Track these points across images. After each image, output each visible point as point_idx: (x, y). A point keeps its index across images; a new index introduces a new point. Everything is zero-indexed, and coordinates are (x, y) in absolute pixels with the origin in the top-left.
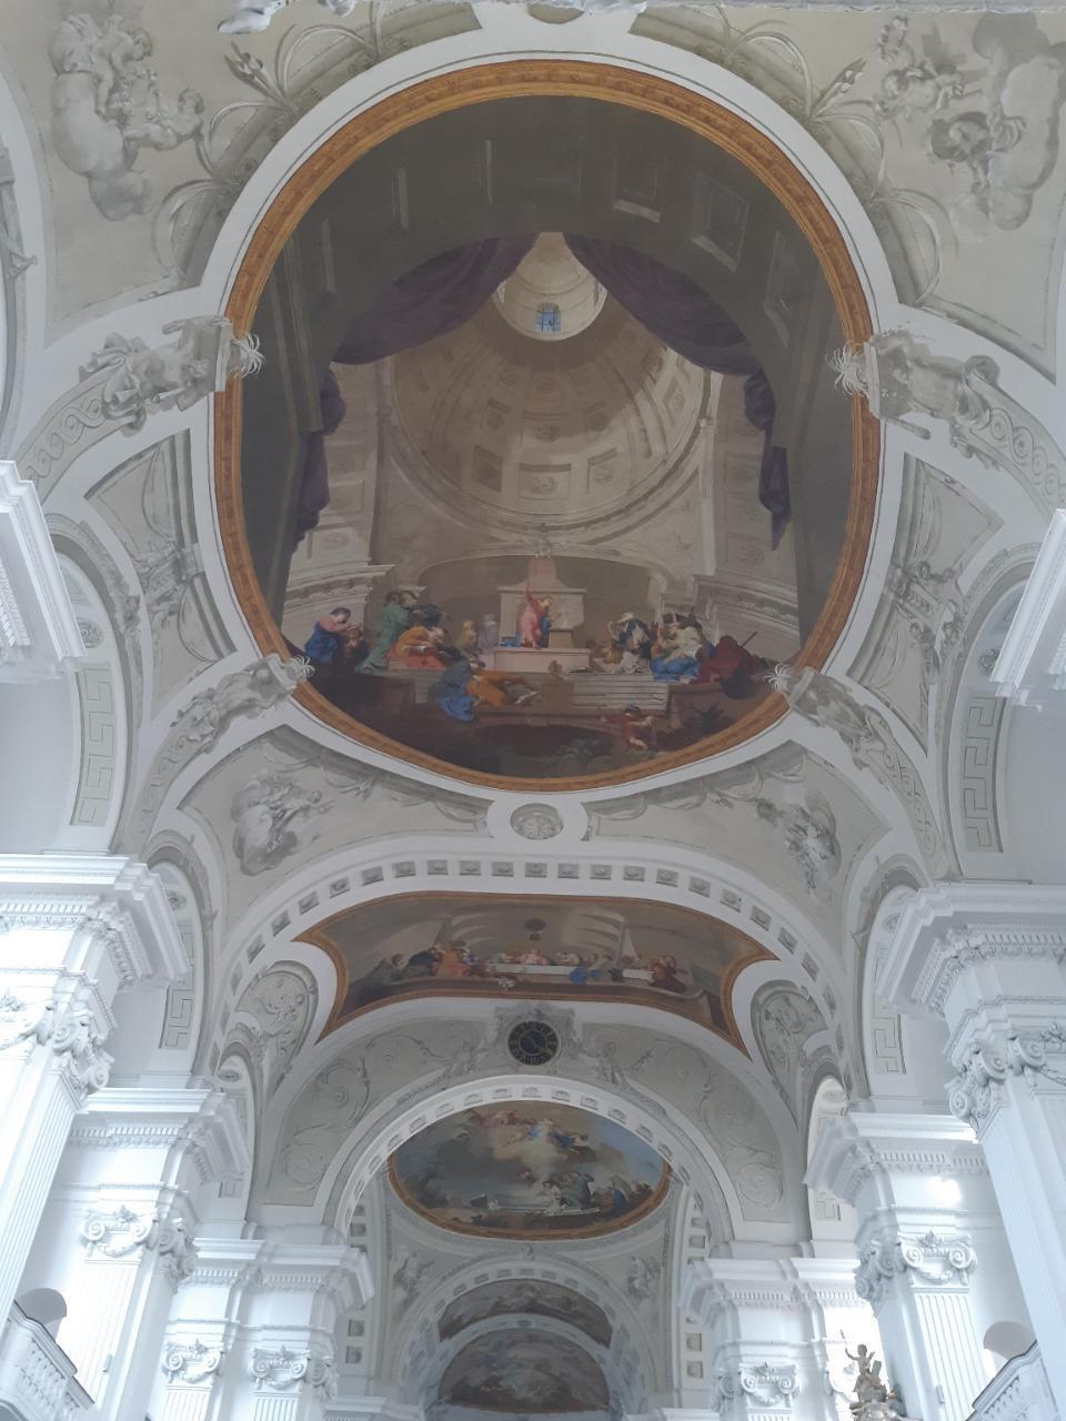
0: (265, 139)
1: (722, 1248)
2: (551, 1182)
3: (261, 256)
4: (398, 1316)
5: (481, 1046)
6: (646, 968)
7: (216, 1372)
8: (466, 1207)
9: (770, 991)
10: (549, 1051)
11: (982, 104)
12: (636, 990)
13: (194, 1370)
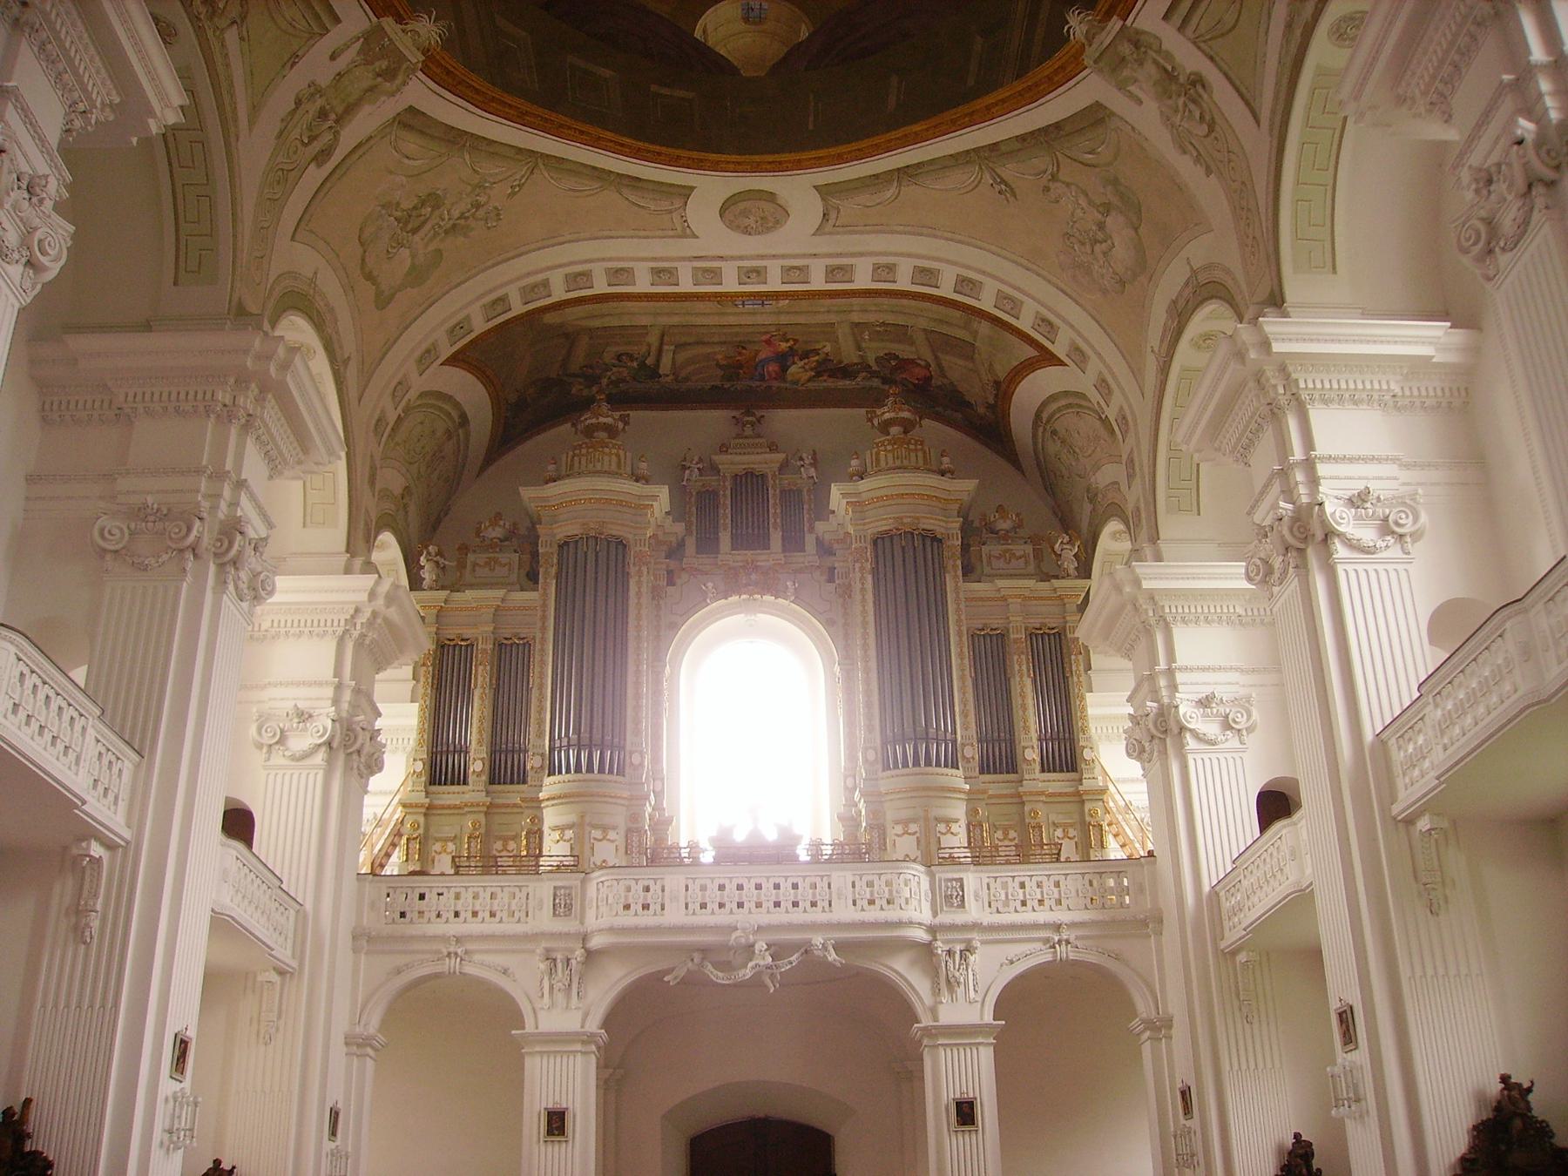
0: (1003, 148)
3: (1037, 85)
11: (417, 238)
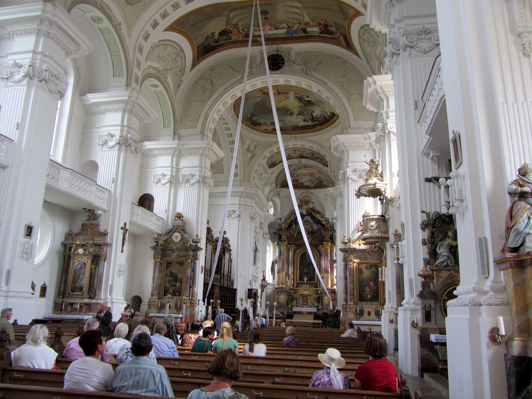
1: (345, 131)
2: (299, 114)
4: (249, 162)
5: (255, 65)
6: (316, 26)
7: (170, 182)
9: (364, 30)
10: (281, 65)
12: (314, 36)
13: (163, 181)
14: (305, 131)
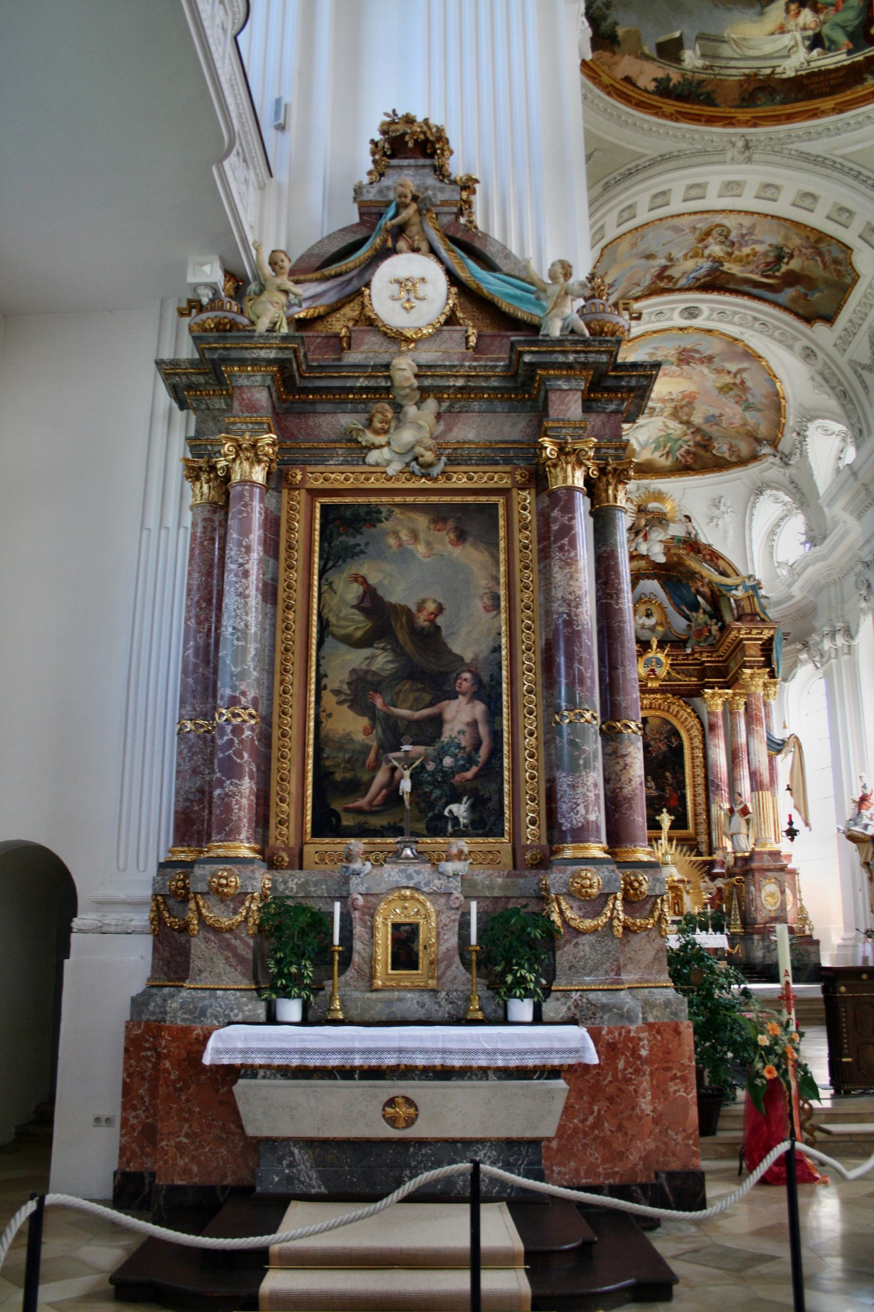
8: (646, 57)
14: (799, 107)
